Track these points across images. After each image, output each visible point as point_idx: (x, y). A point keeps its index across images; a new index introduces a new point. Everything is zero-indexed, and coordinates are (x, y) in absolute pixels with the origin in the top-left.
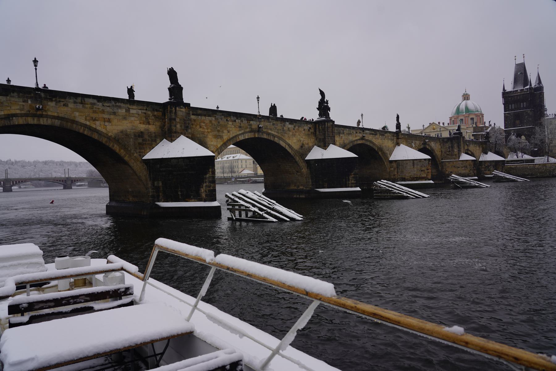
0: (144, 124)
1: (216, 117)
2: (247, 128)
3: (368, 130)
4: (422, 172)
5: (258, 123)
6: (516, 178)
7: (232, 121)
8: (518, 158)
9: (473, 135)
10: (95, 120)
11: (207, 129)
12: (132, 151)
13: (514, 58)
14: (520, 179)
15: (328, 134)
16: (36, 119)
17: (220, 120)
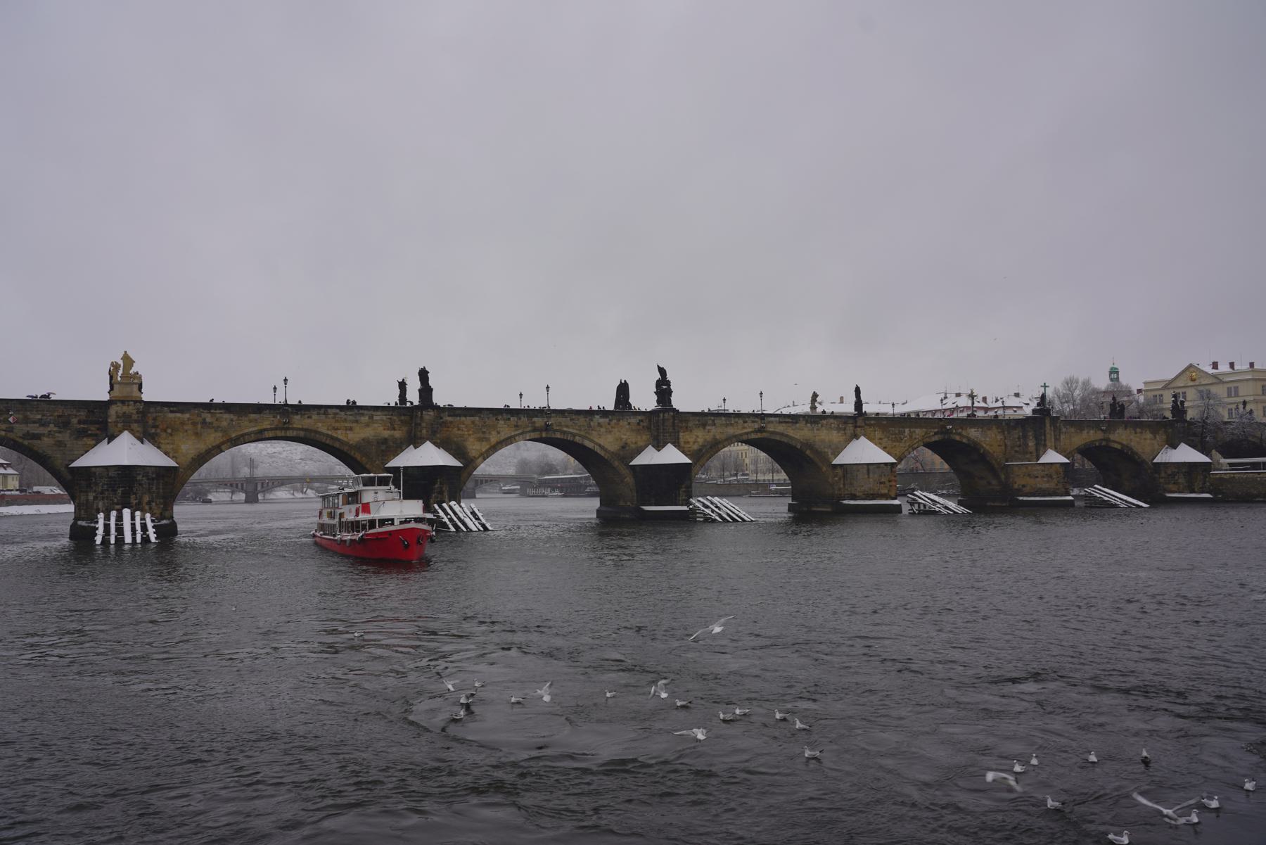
0: (388, 430)
2: (528, 426)
5: (546, 420)
10: (337, 429)
11: (468, 431)
12: (374, 459)
15: (664, 429)
16: (283, 432)
17: (487, 419)
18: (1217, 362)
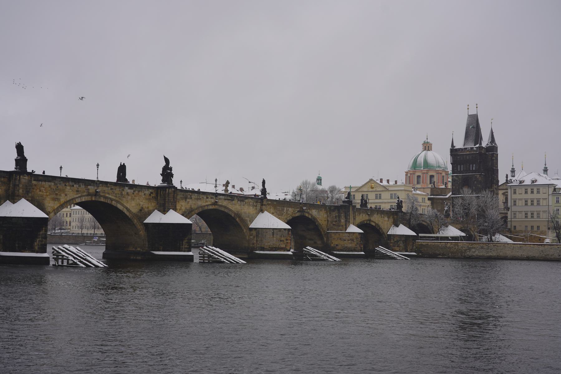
1: (55, 182)
2: (85, 192)
4: (282, 242)
5: (96, 188)
7: (70, 186)
9: (429, 199)
11: (46, 193)
15: (168, 200)
17: (59, 185)
18: (382, 179)
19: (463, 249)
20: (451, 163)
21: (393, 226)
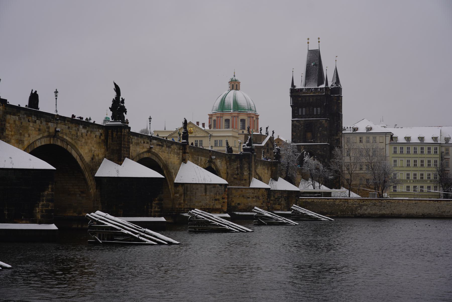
1: (19, 116)
3: (156, 140)
4: (217, 202)
6: (319, 216)
8: (314, 188)
13: (307, 41)
14: (324, 218)
17: (23, 120)
19: (354, 207)
20: (291, 106)
21: (272, 180)
